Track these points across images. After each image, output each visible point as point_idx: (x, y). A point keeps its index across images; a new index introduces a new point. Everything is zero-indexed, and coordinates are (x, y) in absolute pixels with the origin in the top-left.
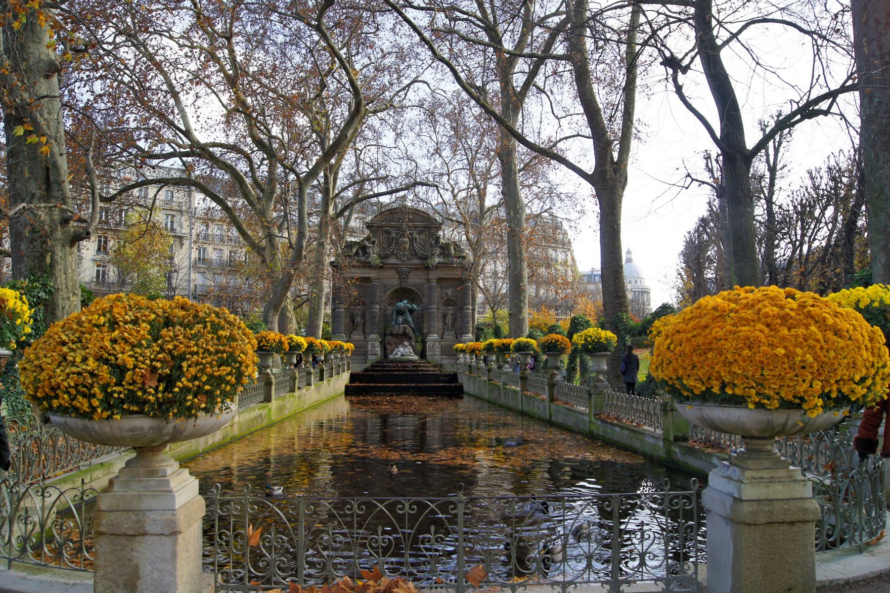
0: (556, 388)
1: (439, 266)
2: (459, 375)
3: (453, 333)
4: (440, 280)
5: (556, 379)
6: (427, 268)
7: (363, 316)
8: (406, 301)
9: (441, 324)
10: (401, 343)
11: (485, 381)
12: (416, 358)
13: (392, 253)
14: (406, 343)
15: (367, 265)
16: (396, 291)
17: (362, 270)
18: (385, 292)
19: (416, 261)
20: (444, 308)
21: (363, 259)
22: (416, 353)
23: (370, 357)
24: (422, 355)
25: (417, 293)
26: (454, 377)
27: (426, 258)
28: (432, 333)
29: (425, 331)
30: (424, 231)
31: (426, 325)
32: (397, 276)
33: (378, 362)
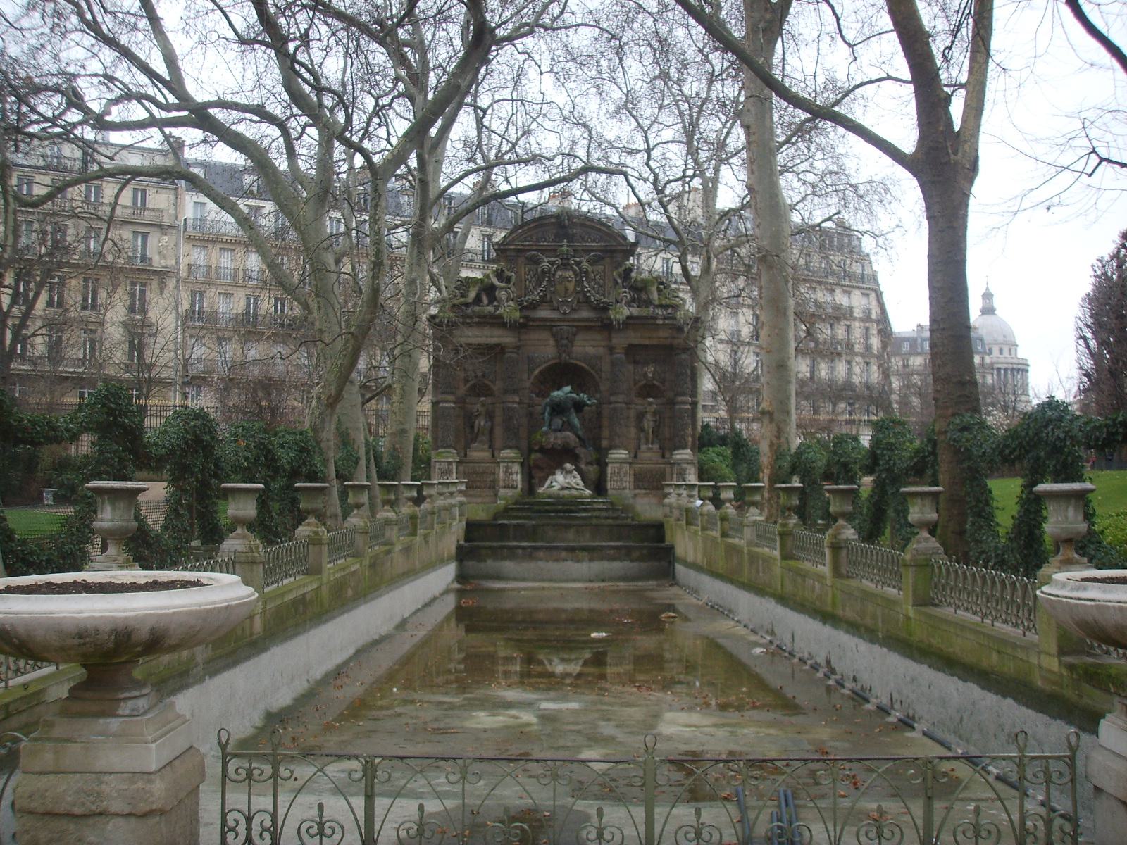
0: (844, 552)
1: (630, 322)
2: (665, 526)
3: (656, 446)
4: (631, 350)
5: (843, 537)
6: (607, 327)
7: (490, 416)
8: (568, 389)
9: (633, 430)
10: (559, 466)
11: (714, 539)
12: (588, 492)
13: (543, 300)
14: (568, 466)
15: (496, 321)
16: (549, 369)
17: (487, 331)
18: (531, 371)
19: (585, 314)
20: (639, 401)
21: (490, 309)
22: (586, 486)
23: (502, 492)
24: (599, 487)
26: (656, 531)
27: (606, 308)
28: (616, 447)
29: (605, 443)
30: (603, 258)
31: (605, 433)
32: (552, 342)
33: (516, 503)
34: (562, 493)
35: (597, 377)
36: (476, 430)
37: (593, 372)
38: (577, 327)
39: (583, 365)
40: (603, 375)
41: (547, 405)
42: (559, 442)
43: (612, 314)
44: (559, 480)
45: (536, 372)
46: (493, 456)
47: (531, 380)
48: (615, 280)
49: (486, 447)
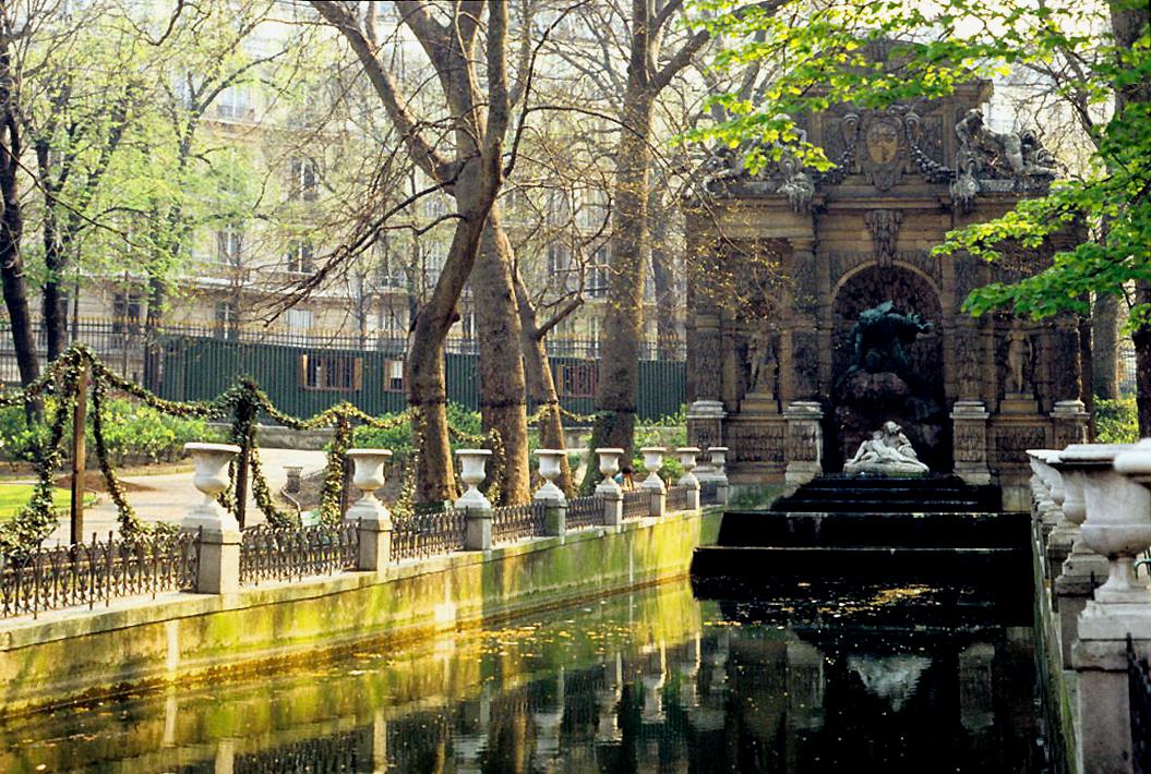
7: (775, 348)
10: (878, 425)
14: (891, 425)
16: (862, 276)
17: (766, 219)
18: (834, 279)
25: (924, 282)
29: (949, 389)
32: (866, 235)
34: (879, 466)
35: (935, 286)
36: (753, 372)
37: (931, 281)
38: (901, 210)
39: (913, 268)
40: (944, 282)
41: (856, 331)
42: (876, 387)
43: (953, 190)
44: (877, 443)
45: (843, 280)
46: (780, 411)
47: (834, 295)
48: (959, 139)
49: (771, 396)
